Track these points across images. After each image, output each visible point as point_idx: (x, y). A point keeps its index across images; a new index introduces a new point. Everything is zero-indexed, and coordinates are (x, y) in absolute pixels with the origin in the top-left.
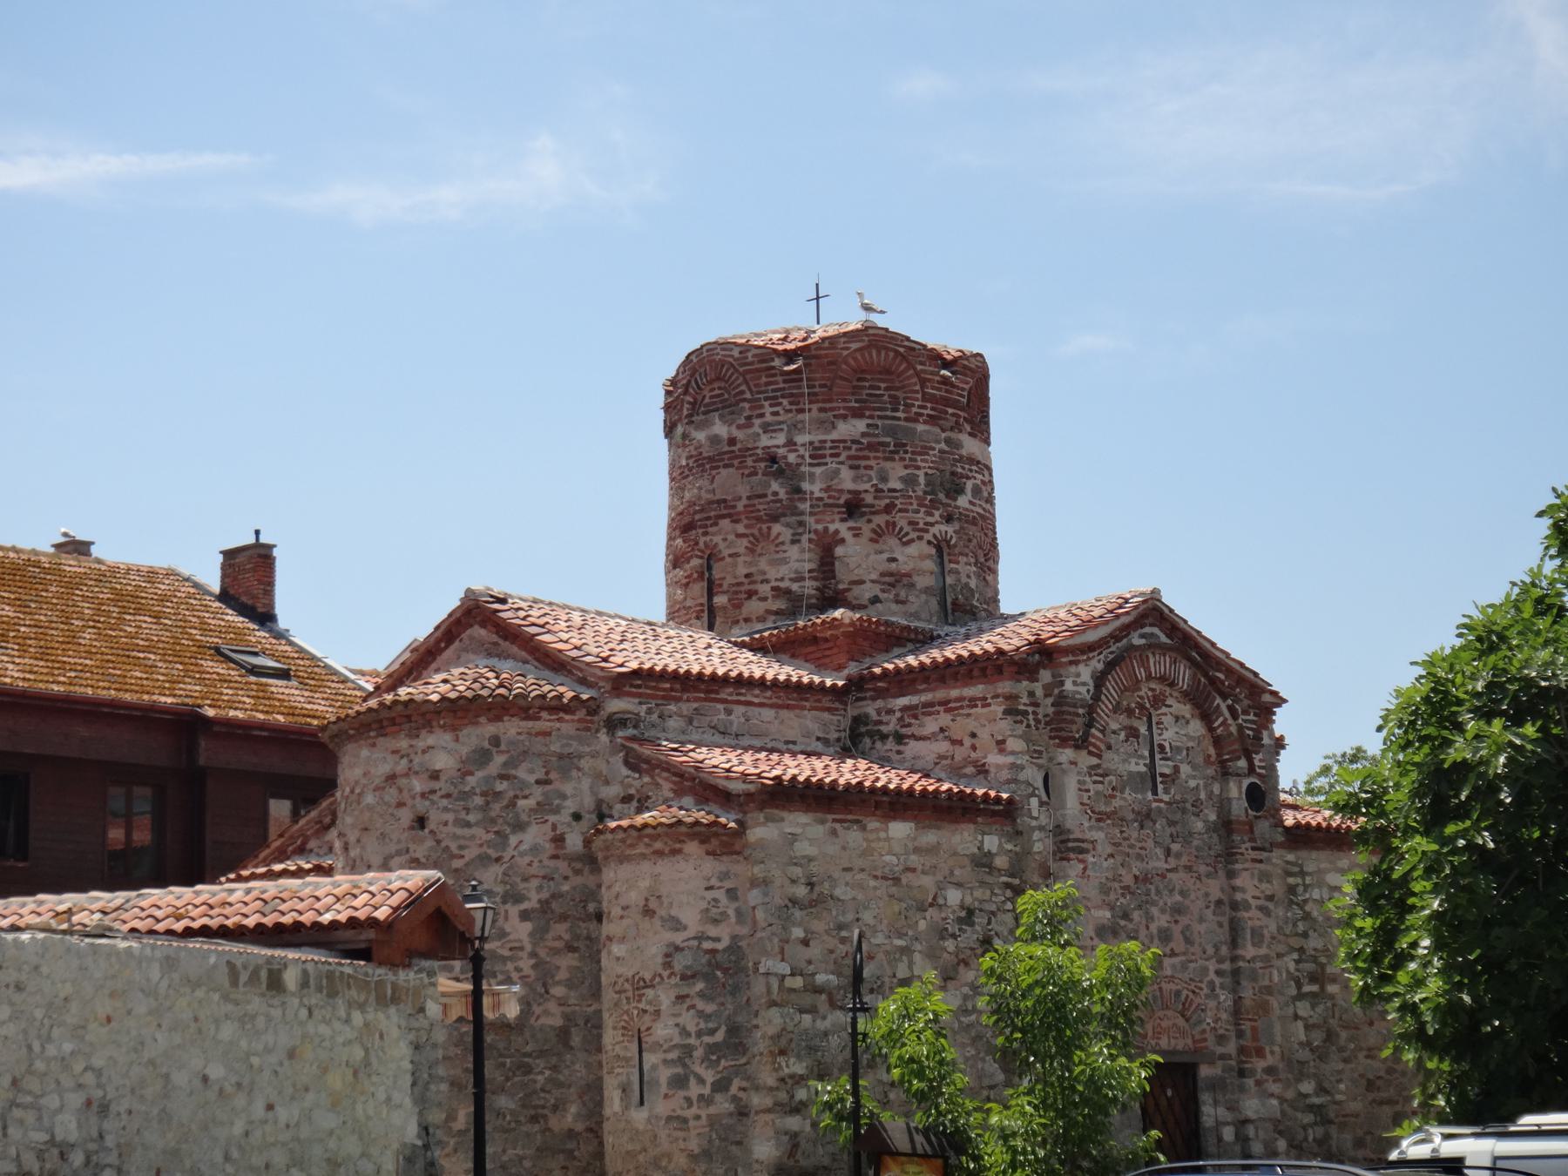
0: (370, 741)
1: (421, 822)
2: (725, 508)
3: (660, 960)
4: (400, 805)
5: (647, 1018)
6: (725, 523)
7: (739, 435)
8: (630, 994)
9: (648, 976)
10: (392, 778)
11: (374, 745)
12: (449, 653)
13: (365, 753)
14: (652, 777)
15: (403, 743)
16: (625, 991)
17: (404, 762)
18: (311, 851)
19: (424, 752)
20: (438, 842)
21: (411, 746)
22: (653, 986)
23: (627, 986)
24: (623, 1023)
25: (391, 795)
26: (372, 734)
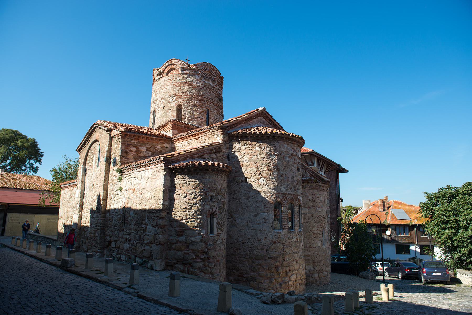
0: (287, 143)
2: (212, 101)
5: (325, 225)
6: (212, 104)
7: (215, 87)
8: (322, 220)
10: (292, 155)
12: (255, 120)
13: (286, 146)
14: (306, 171)
18: (205, 158)
23: (322, 218)
26: (289, 141)
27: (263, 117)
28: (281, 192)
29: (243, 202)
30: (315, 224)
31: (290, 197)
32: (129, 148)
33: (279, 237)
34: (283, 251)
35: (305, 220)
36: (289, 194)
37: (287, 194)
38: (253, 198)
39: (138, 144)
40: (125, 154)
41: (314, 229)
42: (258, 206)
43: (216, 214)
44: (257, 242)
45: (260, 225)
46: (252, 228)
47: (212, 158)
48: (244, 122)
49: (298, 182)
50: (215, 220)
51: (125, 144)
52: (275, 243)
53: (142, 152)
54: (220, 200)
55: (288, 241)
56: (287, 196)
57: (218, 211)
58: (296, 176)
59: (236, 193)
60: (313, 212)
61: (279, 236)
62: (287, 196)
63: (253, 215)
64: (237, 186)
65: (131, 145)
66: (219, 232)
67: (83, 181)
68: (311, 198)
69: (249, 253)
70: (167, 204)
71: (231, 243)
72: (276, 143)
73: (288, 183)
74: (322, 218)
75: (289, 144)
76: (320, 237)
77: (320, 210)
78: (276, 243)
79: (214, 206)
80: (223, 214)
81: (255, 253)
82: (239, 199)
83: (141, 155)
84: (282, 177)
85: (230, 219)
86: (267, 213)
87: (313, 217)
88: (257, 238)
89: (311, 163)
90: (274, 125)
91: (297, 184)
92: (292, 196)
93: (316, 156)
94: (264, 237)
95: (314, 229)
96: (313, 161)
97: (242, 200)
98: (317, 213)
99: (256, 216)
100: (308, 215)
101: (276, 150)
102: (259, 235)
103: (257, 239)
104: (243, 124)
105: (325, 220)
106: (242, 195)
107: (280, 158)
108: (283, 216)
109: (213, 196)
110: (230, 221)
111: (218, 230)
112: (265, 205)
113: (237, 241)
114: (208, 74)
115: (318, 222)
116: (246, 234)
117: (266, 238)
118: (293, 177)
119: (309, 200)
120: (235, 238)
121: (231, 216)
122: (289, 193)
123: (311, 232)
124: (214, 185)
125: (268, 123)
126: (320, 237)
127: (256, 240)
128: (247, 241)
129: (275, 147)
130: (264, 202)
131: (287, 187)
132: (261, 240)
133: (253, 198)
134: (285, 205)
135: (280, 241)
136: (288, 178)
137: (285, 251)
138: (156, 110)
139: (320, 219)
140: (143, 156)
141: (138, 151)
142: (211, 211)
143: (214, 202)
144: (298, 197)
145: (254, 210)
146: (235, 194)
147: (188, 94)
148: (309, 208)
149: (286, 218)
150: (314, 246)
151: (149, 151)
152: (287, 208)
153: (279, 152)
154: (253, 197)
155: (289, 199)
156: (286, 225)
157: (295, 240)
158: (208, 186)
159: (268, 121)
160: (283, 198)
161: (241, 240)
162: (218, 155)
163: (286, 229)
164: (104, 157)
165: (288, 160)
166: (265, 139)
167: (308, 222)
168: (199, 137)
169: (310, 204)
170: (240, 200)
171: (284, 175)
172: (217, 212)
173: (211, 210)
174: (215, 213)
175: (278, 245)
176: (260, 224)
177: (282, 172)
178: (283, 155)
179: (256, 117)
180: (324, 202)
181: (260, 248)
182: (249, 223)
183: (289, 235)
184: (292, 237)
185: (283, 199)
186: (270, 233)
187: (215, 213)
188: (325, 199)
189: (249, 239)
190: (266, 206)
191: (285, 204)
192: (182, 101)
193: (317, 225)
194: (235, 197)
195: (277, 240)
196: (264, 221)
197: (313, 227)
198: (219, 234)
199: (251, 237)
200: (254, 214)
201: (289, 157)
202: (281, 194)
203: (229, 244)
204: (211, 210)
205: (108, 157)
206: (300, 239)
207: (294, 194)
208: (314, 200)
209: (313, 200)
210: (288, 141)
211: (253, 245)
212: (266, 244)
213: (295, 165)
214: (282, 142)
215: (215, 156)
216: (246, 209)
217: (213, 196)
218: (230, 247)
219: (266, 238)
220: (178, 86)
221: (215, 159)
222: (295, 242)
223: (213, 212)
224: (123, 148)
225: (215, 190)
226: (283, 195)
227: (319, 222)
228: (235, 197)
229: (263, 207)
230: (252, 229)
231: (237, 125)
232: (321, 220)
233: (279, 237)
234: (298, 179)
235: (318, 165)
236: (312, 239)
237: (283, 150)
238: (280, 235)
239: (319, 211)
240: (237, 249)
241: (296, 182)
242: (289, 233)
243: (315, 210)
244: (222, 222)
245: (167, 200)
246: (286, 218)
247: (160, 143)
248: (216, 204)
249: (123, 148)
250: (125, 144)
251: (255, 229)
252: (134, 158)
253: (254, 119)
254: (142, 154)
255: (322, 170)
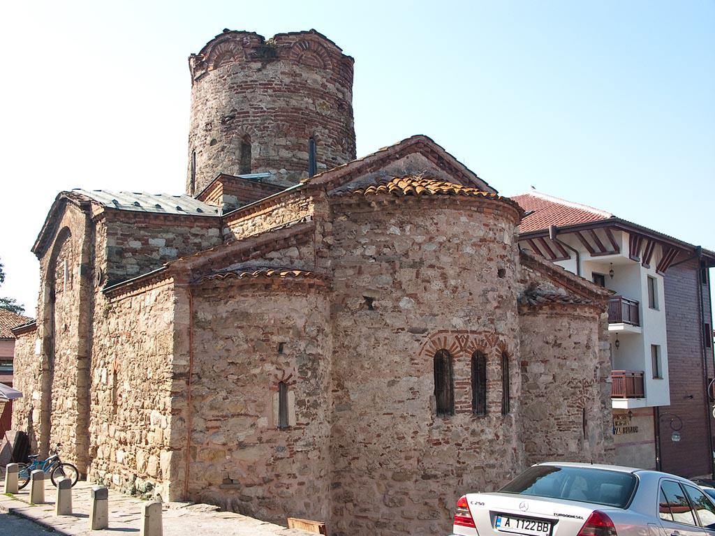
0: (469, 212)
1: (501, 273)
2: (322, 119)
3: (593, 373)
4: (490, 259)
5: (590, 402)
8: (581, 389)
9: (589, 381)
10: (483, 240)
11: (472, 216)
13: (464, 219)
15: (492, 222)
16: (579, 387)
17: (491, 232)
19: (501, 231)
20: (509, 288)
21: (495, 225)
22: (591, 386)
24: (578, 404)
25: (484, 251)
26: (473, 208)
27: (421, 152)
28: (451, 329)
29: (364, 353)
30: (562, 399)
31: (475, 339)
32: (126, 242)
33: (446, 431)
34: (459, 462)
35: (538, 390)
36: (473, 332)
37: (467, 332)
38: (386, 344)
39: (146, 234)
40: (118, 257)
41: (558, 412)
42: (396, 362)
43: (294, 382)
44: (397, 441)
45: (402, 404)
46: (385, 411)
47: (290, 256)
48: (368, 170)
49: (499, 302)
50: (291, 396)
51: (116, 234)
52: (438, 443)
53: (154, 249)
54: (305, 350)
55: (472, 439)
56: (468, 336)
57: (298, 375)
58: (493, 290)
59: (349, 333)
60: (556, 370)
61: (448, 428)
62: (468, 336)
63: (386, 382)
64: (351, 317)
65: (129, 236)
66: (303, 420)
67: (50, 317)
68: (551, 338)
69: (379, 466)
70: (184, 362)
71: (341, 446)
72: (438, 214)
73: (470, 307)
74: (581, 385)
75: (474, 214)
76: (575, 429)
77: (575, 365)
78: (440, 443)
79: (288, 364)
80: (313, 381)
81: (392, 465)
82: (355, 348)
83: (153, 256)
84: (454, 292)
85: (337, 393)
86: (418, 377)
87: (557, 384)
88: (396, 433)
89: (611, 248)
90: (451, 169)
91: (496, 308)
92: (483, 337)
93: (626, 231)
94: (412, 431)
95: (558, 412)
96: (617, 241)
97: (362, 349)
98: (568, 374)
99: (391, 384)
100: (543, 378)
101: (438, 230)
102: (400, 426)
103: (396, 437)
104: (367, 174)
105: (590, 388)
106: (362, 339)
107: (449, 249)
108: (458, 383)
109: (285, 343)
110: (338, 398)
111: (300, 416)
112: (412, 359)
113: (353, 441)
114: (310, 56)
115: (569, 395)
116: (372, 424)
117: (416, 432)
118: (485, 292)
119: (547, 343)
120: (348, 434)
121: (340, 386)
122: (474, 329)
123: (552, 419)
124: (287, 318)
125: (435, 166)
126: (575, 429)
127: (393, 437)
128: (375, 441)
129: (436, 224)
130: (411, 353)
131: (467, 316)
132: (404, 438)
133: (386, 344)
134: (462, 358)
135: (450, 441)
136: (471, 294)
137: (464, 463)
138: (197, 151)
139: (575, 387)
140: (158, 258)
141: (147, 249)
142: (280, 376)
143: (286, 356)
144: (498, 338)
145: (388, 371)
146: (347, 335)
147: (262, 108)
148: (545, 361)
149: (466, 388)
150: (560, 452)
151: (172, 246)
152: (468, 365)
153: (445, 234)
154: (387, 341)
155: (472, 342)
156: (465, 402)
157: (491, 437)
158: (272, 321)
159: (436, 161)
160: (457, 342)
161: (360, 437)
162: (304, 250)
163: (466, 411)
164: (79, 264)
165: (470, 252)
166: (410, 208)
167: (543, 396)
168: (270, 209)
169: (550, 352)
170: (358, 349)
171: (460, 289)
172: (296, 379)
173: (280, 374)
174: (290, 381)
175: (445, 447)
176: (403, 401)
177: (453, 282)
178: (456, 242)
179: (402, 156)
180: (588, 347)
181: (403, 455)
182: (377, 400)
183: (474, 426)
184: (482, 431)
185: (457, 344)
186: (426, 423)
187: (290, 381)
188: (589, 339)
189: (379, 436)
190: (416, 361)
191: (462, 356)
192: (250, 127)
193: (566, 401)
194: (346, 343)
195: (442, 436)
196: (411, 396)
197: (557, 407)
198: (303, 426)
199: (382, 432)
200: (389, 379)
201: (474, 245)
202: (452, 332)
203: (337, 447)
204: (280, 374)
205: (86, 264)
206: (505, 436)
207: (485, 332)
208: (558, 342)
209: (556, 342)
210: (468, 207)
211: (387, 450)
212: (416, 447)
213: (491, 264)
214: (454, 211)
215: (297, 252)
216: (370, 368)
217: (285, 343)
218: (339, 455)
219: (416, 432)
220: (239, 90)
221: (297, 258)
222: (491, 441)
223: (285, 378)
224: (113, 244)
225: (291, 328)
226: (456, 334)
227: (574, 394)
228: (346, 343)
229: (407, 364)
230: (384, 414)
231: (351, 179)
232: (577, 390)
233: (446, 431)
234: (500, 296)
235: (634, 253)
236: (553, 435)
237: (456, 229)
238: (449, 425)
239: (573, 370)
240: (354, 459)
241: (493, 302)
242: (473, 421)
243: (561, 366)
244: (312, 399)
245: (184, 355)
246: (466, 388)
247: (197, 226)
248: (293, 361)
249: (113, 244)
250: (116, 234)
251: (391, 414)
252: (138, 264)
253: (398, 159)
254: (154, 254)
255: (648, 263)
